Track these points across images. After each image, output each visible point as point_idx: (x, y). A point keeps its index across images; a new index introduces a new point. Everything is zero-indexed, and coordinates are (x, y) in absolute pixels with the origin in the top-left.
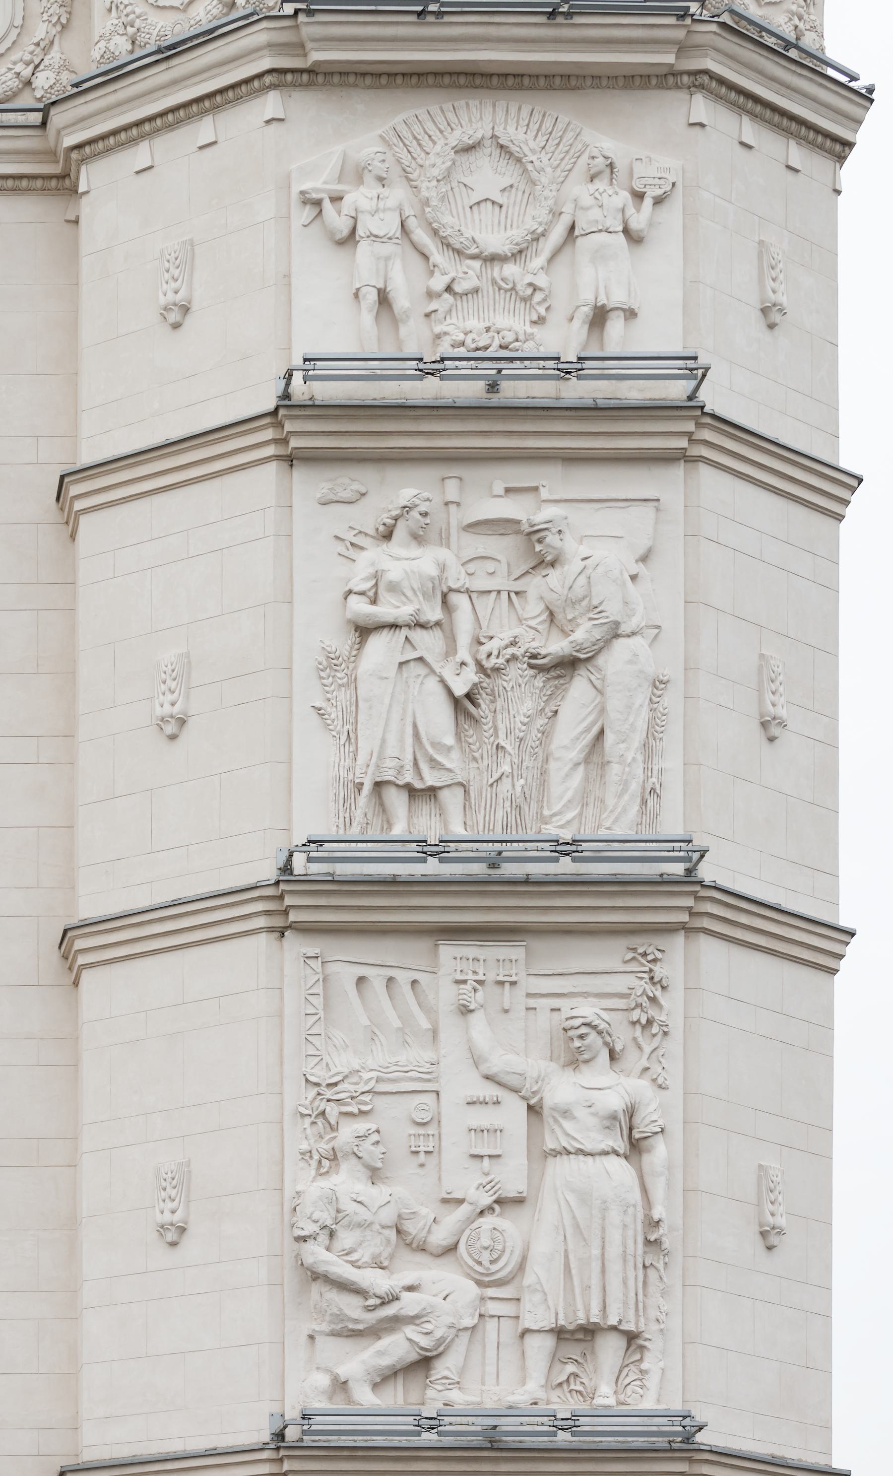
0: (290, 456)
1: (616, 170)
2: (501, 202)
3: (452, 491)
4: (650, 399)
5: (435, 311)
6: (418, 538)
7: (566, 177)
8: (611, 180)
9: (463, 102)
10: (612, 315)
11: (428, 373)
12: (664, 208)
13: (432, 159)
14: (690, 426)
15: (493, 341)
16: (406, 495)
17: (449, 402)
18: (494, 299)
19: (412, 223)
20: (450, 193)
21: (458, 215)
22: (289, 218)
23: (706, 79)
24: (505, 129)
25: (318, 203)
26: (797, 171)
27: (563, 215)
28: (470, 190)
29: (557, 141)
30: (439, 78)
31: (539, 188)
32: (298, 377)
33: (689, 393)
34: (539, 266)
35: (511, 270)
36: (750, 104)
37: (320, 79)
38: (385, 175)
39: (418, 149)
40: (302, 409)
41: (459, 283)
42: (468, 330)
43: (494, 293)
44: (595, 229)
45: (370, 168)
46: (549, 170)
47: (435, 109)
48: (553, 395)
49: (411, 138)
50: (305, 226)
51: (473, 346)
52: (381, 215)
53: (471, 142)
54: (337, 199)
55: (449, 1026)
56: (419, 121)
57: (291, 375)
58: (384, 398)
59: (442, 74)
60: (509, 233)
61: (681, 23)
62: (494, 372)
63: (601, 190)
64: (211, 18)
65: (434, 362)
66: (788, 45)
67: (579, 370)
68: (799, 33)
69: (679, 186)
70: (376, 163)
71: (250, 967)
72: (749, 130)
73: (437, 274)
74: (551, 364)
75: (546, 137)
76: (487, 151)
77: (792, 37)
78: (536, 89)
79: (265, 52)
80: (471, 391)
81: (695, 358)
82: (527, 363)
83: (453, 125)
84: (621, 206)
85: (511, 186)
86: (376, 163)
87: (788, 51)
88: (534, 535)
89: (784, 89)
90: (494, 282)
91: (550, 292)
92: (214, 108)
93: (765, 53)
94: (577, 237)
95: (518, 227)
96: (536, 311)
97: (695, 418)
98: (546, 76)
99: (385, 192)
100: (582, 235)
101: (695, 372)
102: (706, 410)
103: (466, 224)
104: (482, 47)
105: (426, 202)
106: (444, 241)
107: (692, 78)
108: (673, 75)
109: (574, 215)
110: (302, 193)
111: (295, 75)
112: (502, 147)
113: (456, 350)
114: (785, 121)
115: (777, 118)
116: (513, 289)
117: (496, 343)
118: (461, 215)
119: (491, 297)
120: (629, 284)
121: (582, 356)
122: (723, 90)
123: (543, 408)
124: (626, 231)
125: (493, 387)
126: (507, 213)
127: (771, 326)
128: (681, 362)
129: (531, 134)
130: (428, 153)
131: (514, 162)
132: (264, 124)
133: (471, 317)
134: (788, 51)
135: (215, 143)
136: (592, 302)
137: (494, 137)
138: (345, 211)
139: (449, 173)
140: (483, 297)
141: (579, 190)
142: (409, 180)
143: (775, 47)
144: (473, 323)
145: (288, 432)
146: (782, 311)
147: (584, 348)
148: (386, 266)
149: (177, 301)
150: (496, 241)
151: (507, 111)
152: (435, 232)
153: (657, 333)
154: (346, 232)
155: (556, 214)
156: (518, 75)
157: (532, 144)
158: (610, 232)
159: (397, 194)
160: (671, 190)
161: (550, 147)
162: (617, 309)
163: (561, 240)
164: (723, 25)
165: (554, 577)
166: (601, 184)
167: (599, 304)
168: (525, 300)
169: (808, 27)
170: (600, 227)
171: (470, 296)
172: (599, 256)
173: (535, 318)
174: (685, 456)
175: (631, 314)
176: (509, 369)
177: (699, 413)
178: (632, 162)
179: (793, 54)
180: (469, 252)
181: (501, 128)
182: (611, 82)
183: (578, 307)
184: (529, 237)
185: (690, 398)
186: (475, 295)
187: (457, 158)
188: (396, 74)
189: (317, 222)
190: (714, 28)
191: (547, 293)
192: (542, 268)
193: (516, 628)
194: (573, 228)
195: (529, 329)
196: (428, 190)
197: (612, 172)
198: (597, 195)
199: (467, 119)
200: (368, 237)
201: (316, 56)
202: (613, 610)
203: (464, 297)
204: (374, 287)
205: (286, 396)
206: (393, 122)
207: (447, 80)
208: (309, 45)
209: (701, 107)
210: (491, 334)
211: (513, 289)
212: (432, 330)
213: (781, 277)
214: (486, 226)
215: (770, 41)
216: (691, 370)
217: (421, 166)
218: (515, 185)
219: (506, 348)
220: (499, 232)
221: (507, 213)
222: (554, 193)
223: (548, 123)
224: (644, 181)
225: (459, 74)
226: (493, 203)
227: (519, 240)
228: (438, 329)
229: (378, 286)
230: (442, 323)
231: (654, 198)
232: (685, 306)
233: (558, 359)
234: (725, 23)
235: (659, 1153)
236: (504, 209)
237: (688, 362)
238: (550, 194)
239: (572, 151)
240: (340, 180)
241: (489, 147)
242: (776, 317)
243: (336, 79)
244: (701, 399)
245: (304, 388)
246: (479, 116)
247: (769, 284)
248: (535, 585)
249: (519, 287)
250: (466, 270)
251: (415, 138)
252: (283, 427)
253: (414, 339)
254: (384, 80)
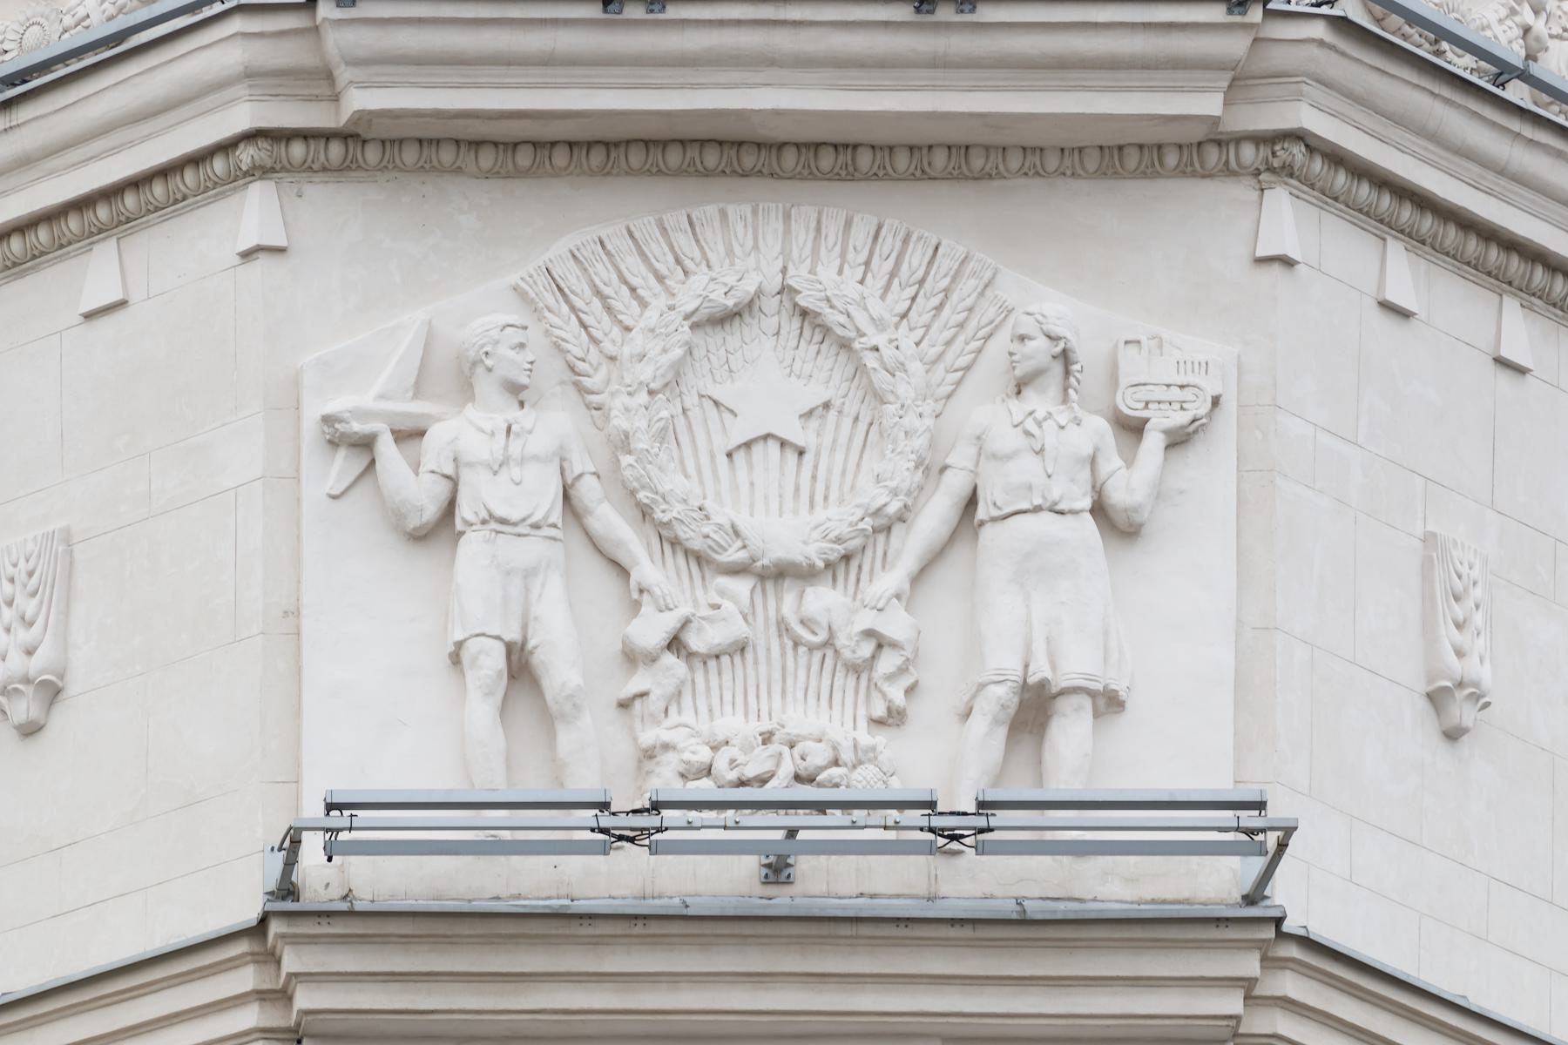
0: (295, 1030)
1: (1076, 367)
2: (801, 443)
4: (1153, 901)
5: (643, 695)
7: (959, 383)
8: (1065, 390)
9: (712, 210)
10: (1063, 704)
11: (621, 838)
12: (1192, 461)
13: (638, 340)
14: (1250, 965)
15: (778, 765)
17: (673, 905)
18: (784, 668)
19: (589, 492)
20: (681, 422)
21: (699, 472)
22: (298, 479)
23: (1298, 152)
24: (812, 271)
25: (365, 444)
26: (1521, 371)
27: (948, 473)
28: (727, 416)
29: (936, 301)
30: (656, 153)
31: (891, 408)
32: (312, 845)
33: (1247, 886)
34: (892, 591)
35: (822, 600)
36: (1406, 213)
37: (372, 154)
38: (524, 380)
39: (606, 318)
40: (324, 921)
41: (700, 629)
42: (721, 738)
43: (783, 654)
44: (1025, 506)
45: (489, 362)
46: (916, 367)
47: (645, 226)
48: (922, 890)
49: (588, 293)
50: (334, 497)
51: (732, 776)
52: (515, 472)
53: (730, 303)
54: (410, 435)
56: (608, 254)
57: (296, 842)
58: (519, 897)
59: (664, 144)
60: (821, 514)
61: (1237, 19)
62: (779, 835)
63: (1040, 414)
64: (112, 10)
65: (635, 812)
66: (1505, 72)
67: (981, 831)
68: (1533, 44)
69: (1230, 405)
70: (504, 351)
72: (1404, 273)
73: (647, 608)
74: (915, 816)
75: (911, 291)
76: (770, 323)
77: (1514, 53)
78: (887, 177)
79: (241, 90)
80: (728, 880)
81: (1260, 806)
82: (859, 815)
83: (688, 263)
84: (1087, 450)
85: (827, 406)
86: (504, 351)
87: (1503, 85)
89: (1490, 176)
90: (783, 627)
91: (916, 651)
92: (120, 223)
93: (1446, 92)
94: (982, 523)
95: (841, 501)
96: (884, 695)
97: (1261, 945)
98: (911, 148)
99: (524, 418)
100: (994, 520)
101: (1261, 837)
102: (1287, 927)
103: (718, 494)
104: (759, 77)
105: (624, 443)
106: (664, 533)
107: (1264, 151)
108: (1219, 143)
109: (975, 473)
110: (328, 420)
111: (312, 144)
112: (804, 313)
113: (691, 785)
114: (1494, 254)
115: (1473, 246)
116: (828, 643)
117: (787, 769)
118: (707, 474)
119: (777, 665)
120: (1106, 633)
121: (989, 798)
122: (1341, 179)
123: (897, 921)
124: (1099, 510)
125: (777, 871)
126: (816, 467)
127: (1453, 735)
128: (1229, 814)
129: (875, 283)
130: (628, 329)
131: (834, 349)
132: (238, 260)
133: (728, 708)
134: (1503, 85)
135: (122, 304)
136: (1016, 674)
137: (786, 290)
138: (429, 463)
139: (678, 374)
140: (756, 662)
141: (989, 414)
142: (582, 390)
143: (1474, 79)
144: (735, 724)
145: (291, 975)
146: (1478, 698)
147: (995, 784)
148: (527, 589)
149: (32, 673)
150: (788, 534)
151: (818, 230)
152: (645, 512)
153: (1173, 748)
154: (431, 512)
155: (932, 470)
156: (846, 146)
157: (876, 307)
158: (1061, 513)
159: (554, 424)
160: (1210, 415)
161: (920, 315)
162: (1075, 690)
163: (945, 532)
164: (1343, 25)
166: (1040, 401)
167: (1031, 680)
168: (856, 669)
169: (1557, 30)
170: (1037, 501)
171: (725, 660)
173: (880, 711)
174: (1236, 1035)
175: (1109, 703)
176: (812, 826)
177: (1270, 933)
178: (1116, 346)
179: (1516, 92)
180: (724, 558)
181: (803, 270)
182: (1067, 162)
183: (982, 686)
184: (867, 524)
185: (1250, 900)
186: (737, 659)
187: (698, 339)
188: (554, 144)
189: (364, 488)
190: (1319, 30)
191: (908, 653)
192: (898, 597)
194: (972, 502)
195: (865, 737)
196: (629, 413)
197: (1067, 373)
198: (1030, 425)
199: (721, 248)
200: (484, 522)
201: (360, 100)
203: (712, 663)
204: (498, 638)
205: (287, 890)
206: (546, 257)
207: (674, 157)
208: (344, 74)
209: (1284, 219)
210: (774, 748)
211: (828, 643)
212: (635, 739)
213: (1478, 619)
214: (766, 497)
215: (1461, 64)
216: (1250, 832)
217: (612, 359)
218: (837, 402)
219: (810, 780)
220: (796, 512)
221: (816, 467)
222: (929, 422)
223: (916, 259)
224: (1143, 393)
225: (703, 143)
226: (783, 444)
227: (845, 530)
228: (649, 737)
229: (507, 638)
230: (658, 723)
231: (1167, 432)
232: (1240, 685)
233: (932, 805)
234: (1344, 19)
236: (808, 457)
237: (1243, 814)
238: (917, 422)
239: (972, 324)
240: (418, 391)
241: (773, 314)
242: (1462, 713)
243: (410, 155)
244: (1277, 903)
245: (329, 872)
246: (750, 243)
247: (1448, 635)
249: (841, 641)
250: (718, 600)
251: (598, 293)
252: (278, 962)
253: (593, 758)
254: (524, 158)
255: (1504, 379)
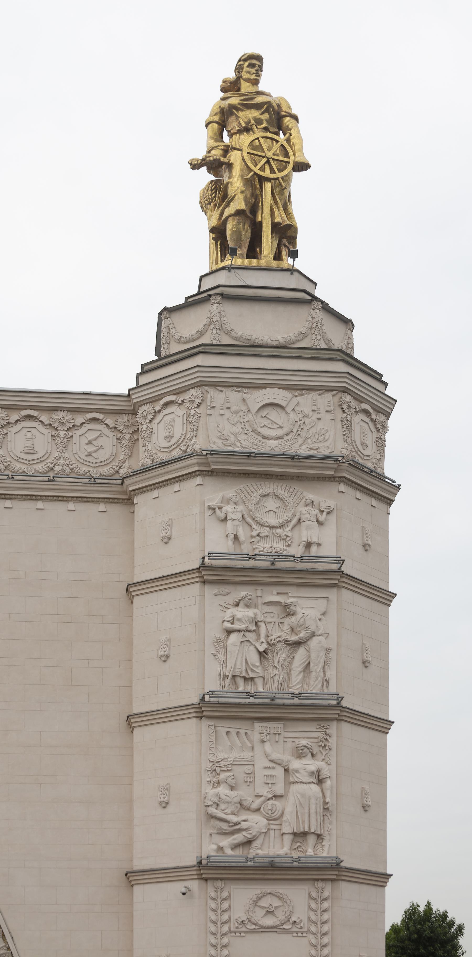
13: (253, 498)
14: (339, 577)
19: (246, 516)
23: (344, 479)
25: (214, 509)
26: (375, 507)
35: (279, 531)
36: (359, 487)
37: (215, 473)
46: (292, 503)
47: (254, 484)
54: (220, 508)
59: (256, 474)
60: (279, 520)
66: (372, 471)
69: (335, 509)
72: (359, 495)
73: (254, 531)
77: (373, 469)
80: (266, 564)
81: (340, 558)
90: (273, 534)
99: (237, 507)
105: (251, 510)
112: (276, 496)
114: (371, 493)
115: (368, 492)
117: (274, 551)
122: (350, 483)
125: (273, 564)
127: (366, 550)
129: (286, 492)
141: (302, 509)
142: (245, 504)
144: (266, 545)
146: (370, 546)
150: (274, 522)
153: (329, 550)
155: (294, 515)
157: (286, 495)
159: (241, 508)
166: (309, 508)
168: (284, 539)
173: (287, 544)
175: (319, 545)
185: (339, 569)
187: (261, 498)
189: (214, 514)
190: (347, 465)
194: (300, 519)
195: (285, 548)
196: (251, 507)
201: (213, 467)
208: (211, 464)
209: (342, 487)
215: (366, 470)
223: (292, 490)
225: (262, 474)
228: (254, 547)
232: (337, 543)
240: (221, 503)
253: (246, 549)
255: (373, 508)
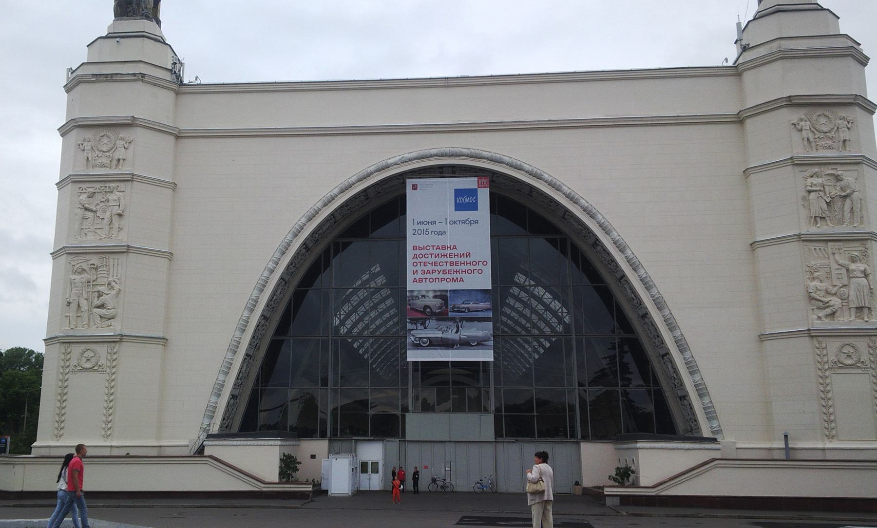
3: (822, 169)
6: (818, 177)
16: (816, 170)
55: (831, 257)
71: (795, 246)
88: (838, 176)
150: (825, 129)
165: (842, 183)
172: (844, 131)
193: (835, 191)
202: (854, 188)
235: (871, 277)
248: (838, 184)
